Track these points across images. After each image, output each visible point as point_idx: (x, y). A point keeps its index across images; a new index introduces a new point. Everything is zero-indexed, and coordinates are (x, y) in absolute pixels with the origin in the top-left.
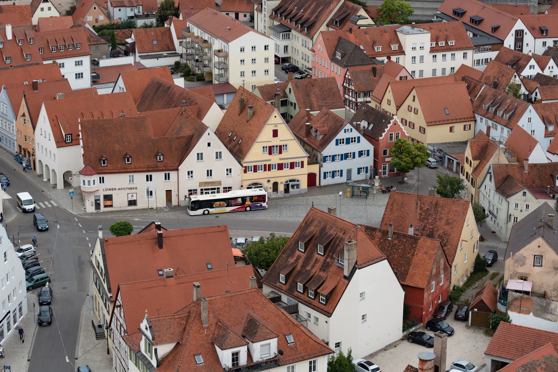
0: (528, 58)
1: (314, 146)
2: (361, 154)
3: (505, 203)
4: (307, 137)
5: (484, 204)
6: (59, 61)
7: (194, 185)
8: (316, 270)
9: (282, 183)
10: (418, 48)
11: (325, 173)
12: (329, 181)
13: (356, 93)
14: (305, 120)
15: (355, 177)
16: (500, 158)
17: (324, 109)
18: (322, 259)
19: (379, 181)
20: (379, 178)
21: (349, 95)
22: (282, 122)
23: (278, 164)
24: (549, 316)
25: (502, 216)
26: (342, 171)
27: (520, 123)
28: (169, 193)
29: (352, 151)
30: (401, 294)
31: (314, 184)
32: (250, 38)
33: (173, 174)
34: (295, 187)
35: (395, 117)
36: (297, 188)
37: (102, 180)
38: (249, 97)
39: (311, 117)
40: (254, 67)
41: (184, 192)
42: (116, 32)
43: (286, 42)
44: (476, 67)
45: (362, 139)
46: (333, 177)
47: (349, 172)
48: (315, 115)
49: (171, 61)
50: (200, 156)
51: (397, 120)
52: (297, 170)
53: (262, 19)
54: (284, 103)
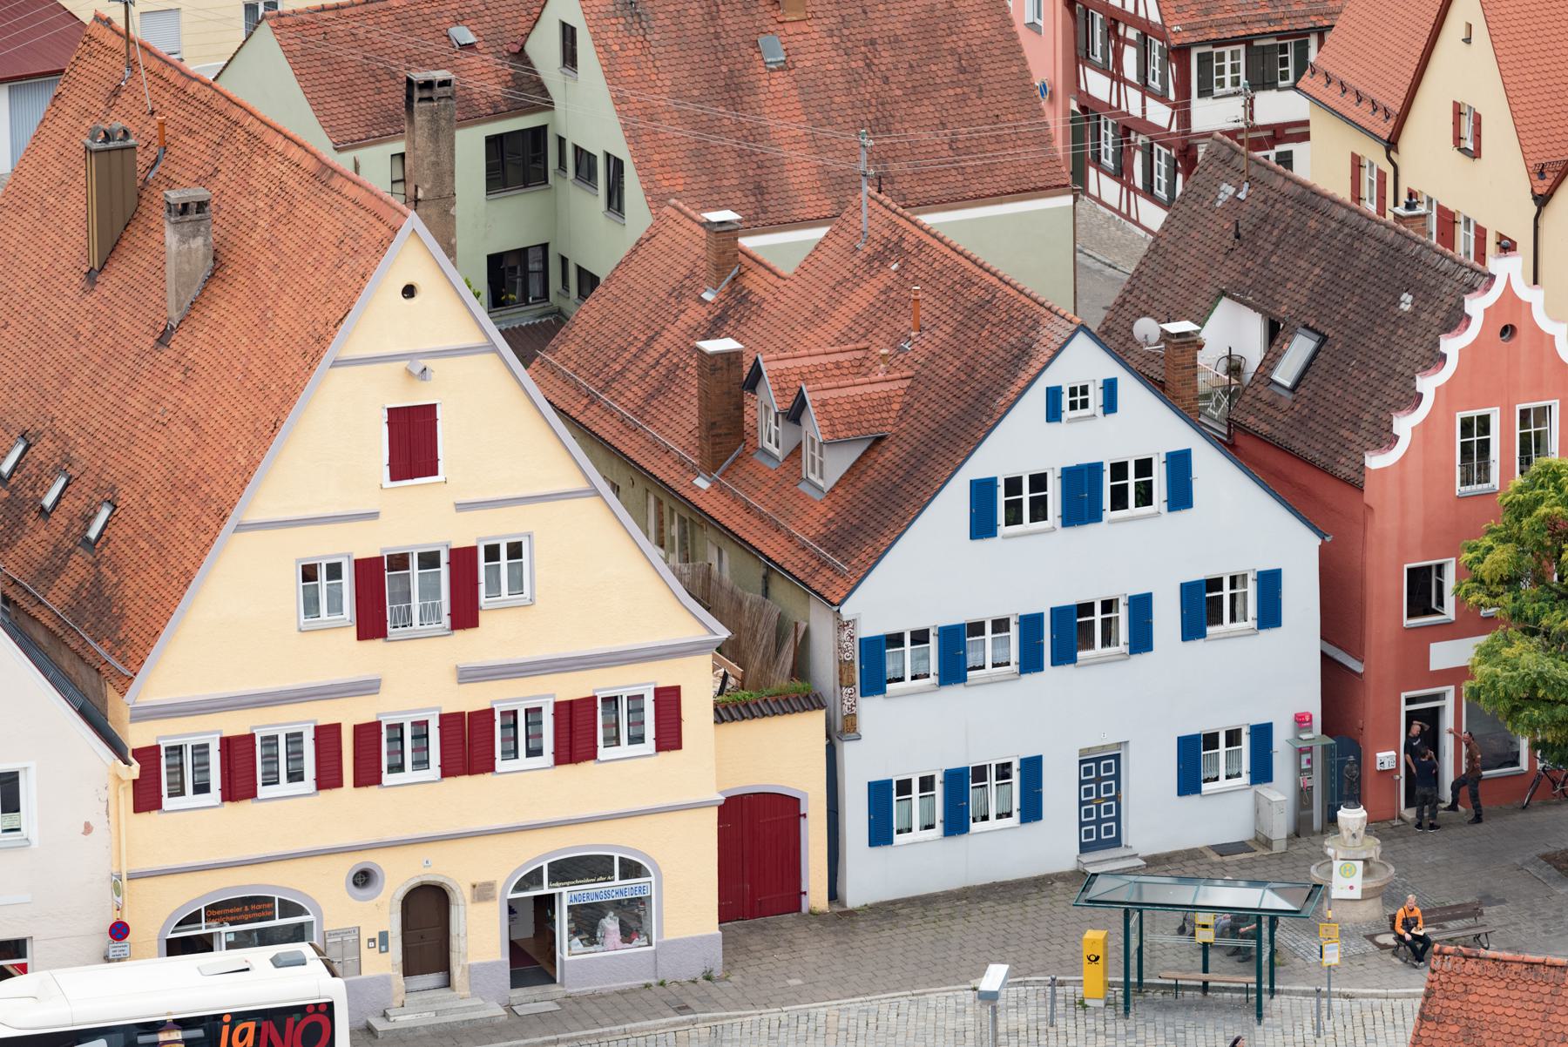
1: (773, 547)
2: (1203, 606)
4: (712, 464)
9: (482, 892)
11: (880, 795)
12: (921, 860)
13: (1180, 53)
14: (695, 315)
15: (1156, 816)
17: (869, 214)
19: (1373, 848)
20: (1374, 826)
21: (1117, 77)
22: (476, 339)
23: (447, 721)
26: (1032, 768)
29: (1123, 589)
31: (791, 897)
34: (611, 924)
35: (1508, 270)
36: (628, 934)
38: (174, 114)
39: (755, 283)
45: (1214, 472)
46: (956, 823)
47: (1102, 772)
48: (787, 267)
51: (1524, 291)
52: (624, 772)
54: (519, 162)
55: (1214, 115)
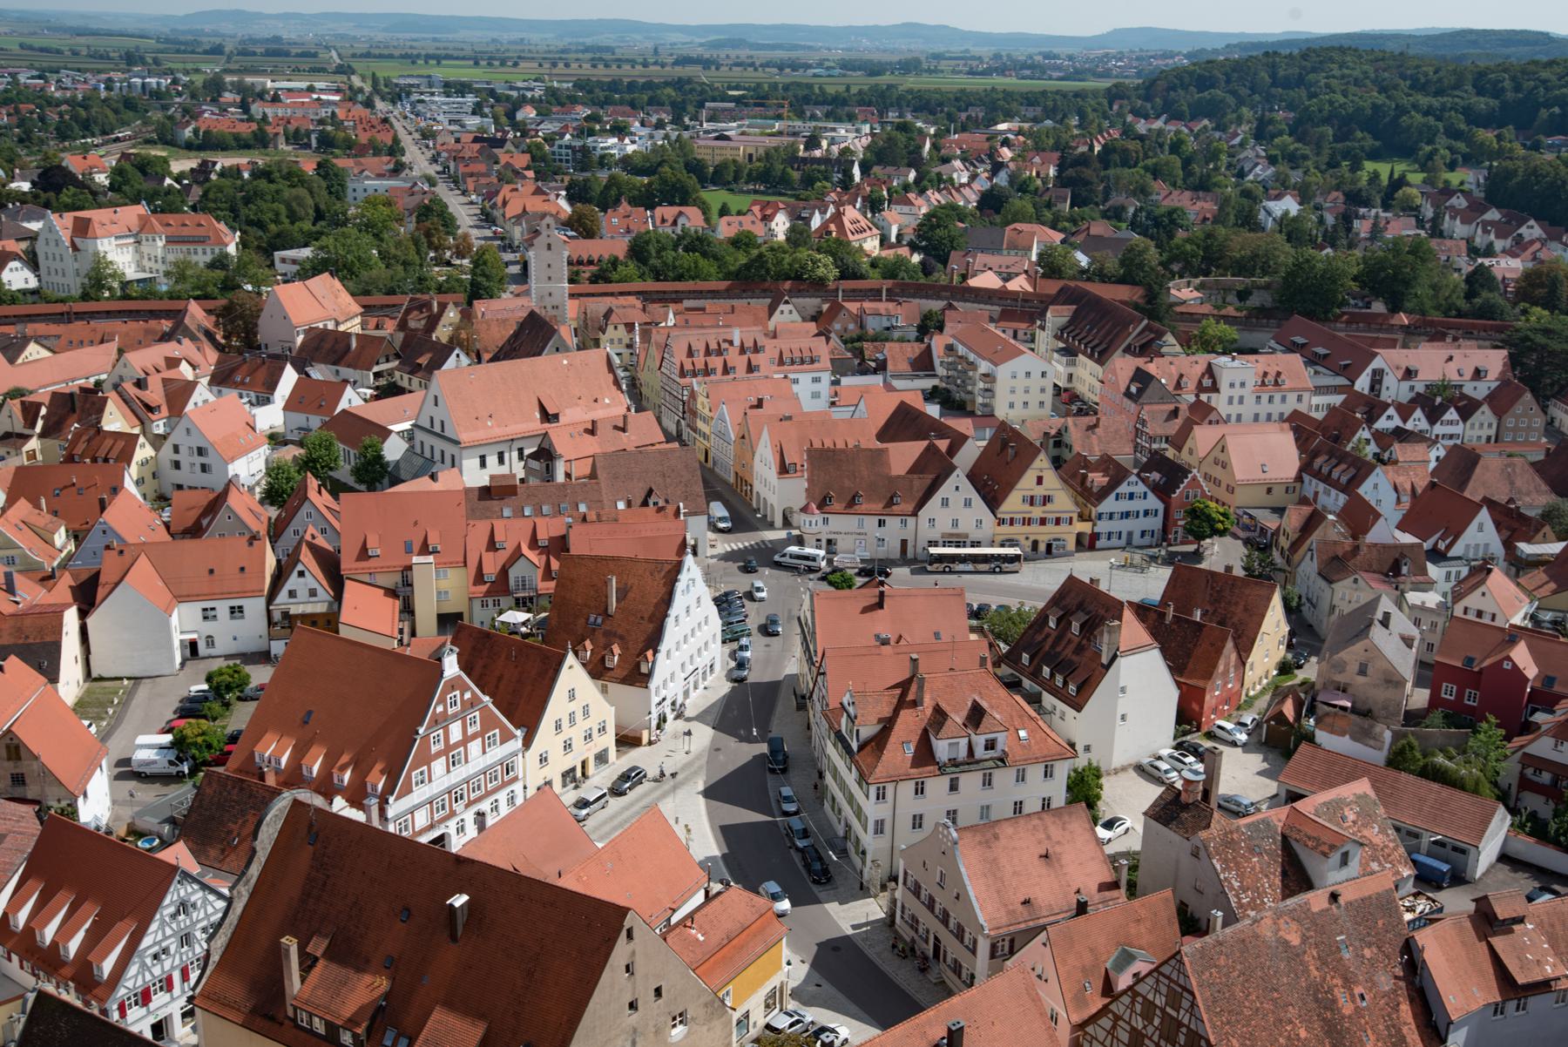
0: (1386, 406)
2: (1146, 513)
3: (1328, 592)
6: (791, 376)
7: (935, 535)
8: (1068, 652)
10: (1237, 385)
18: (1077, 640)
24: (1372, 742)
27: (1361, 491)
28: (904, 542)
30: (1174, 694)
32: (1027, 361)
33: (911, 521)
37: (826, 521)
40: (1026, 398)
41: (922, 543)
42: (865, 345)
43: (1071, 370)
44: (1314, 414)
45: (1150, 494)
47: (1130, 534)
49: (928, 384)
50: (945, 502)
52: (1064, 527)
53: (1045, 338)
55: (1155, 446)
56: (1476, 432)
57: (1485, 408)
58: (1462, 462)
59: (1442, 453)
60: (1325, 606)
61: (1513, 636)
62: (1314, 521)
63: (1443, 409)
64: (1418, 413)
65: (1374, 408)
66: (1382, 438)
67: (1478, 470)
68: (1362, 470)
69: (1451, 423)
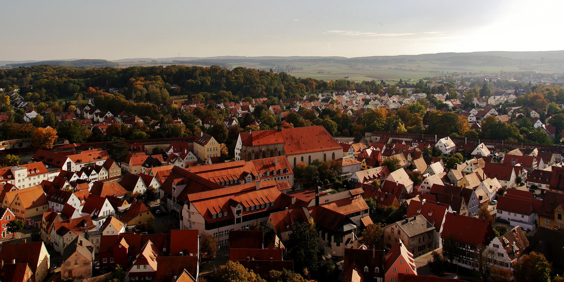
0: (73, 173)
5: (52, 241)
16: (59, 219)
25: (61, 244)
27: (68, 202)
56: (102, 176)
57: (103, 168)
58: (99, 185)
59: (93, 184)
60: (61, 244)
61: (122, 235)
62: (51, 218)
63: (91, 171)
64: (83, 174)
65: (69, 174)
66: (73, 184)
67: (103, 188)
68: (67, 195)
69: (94, 174)
